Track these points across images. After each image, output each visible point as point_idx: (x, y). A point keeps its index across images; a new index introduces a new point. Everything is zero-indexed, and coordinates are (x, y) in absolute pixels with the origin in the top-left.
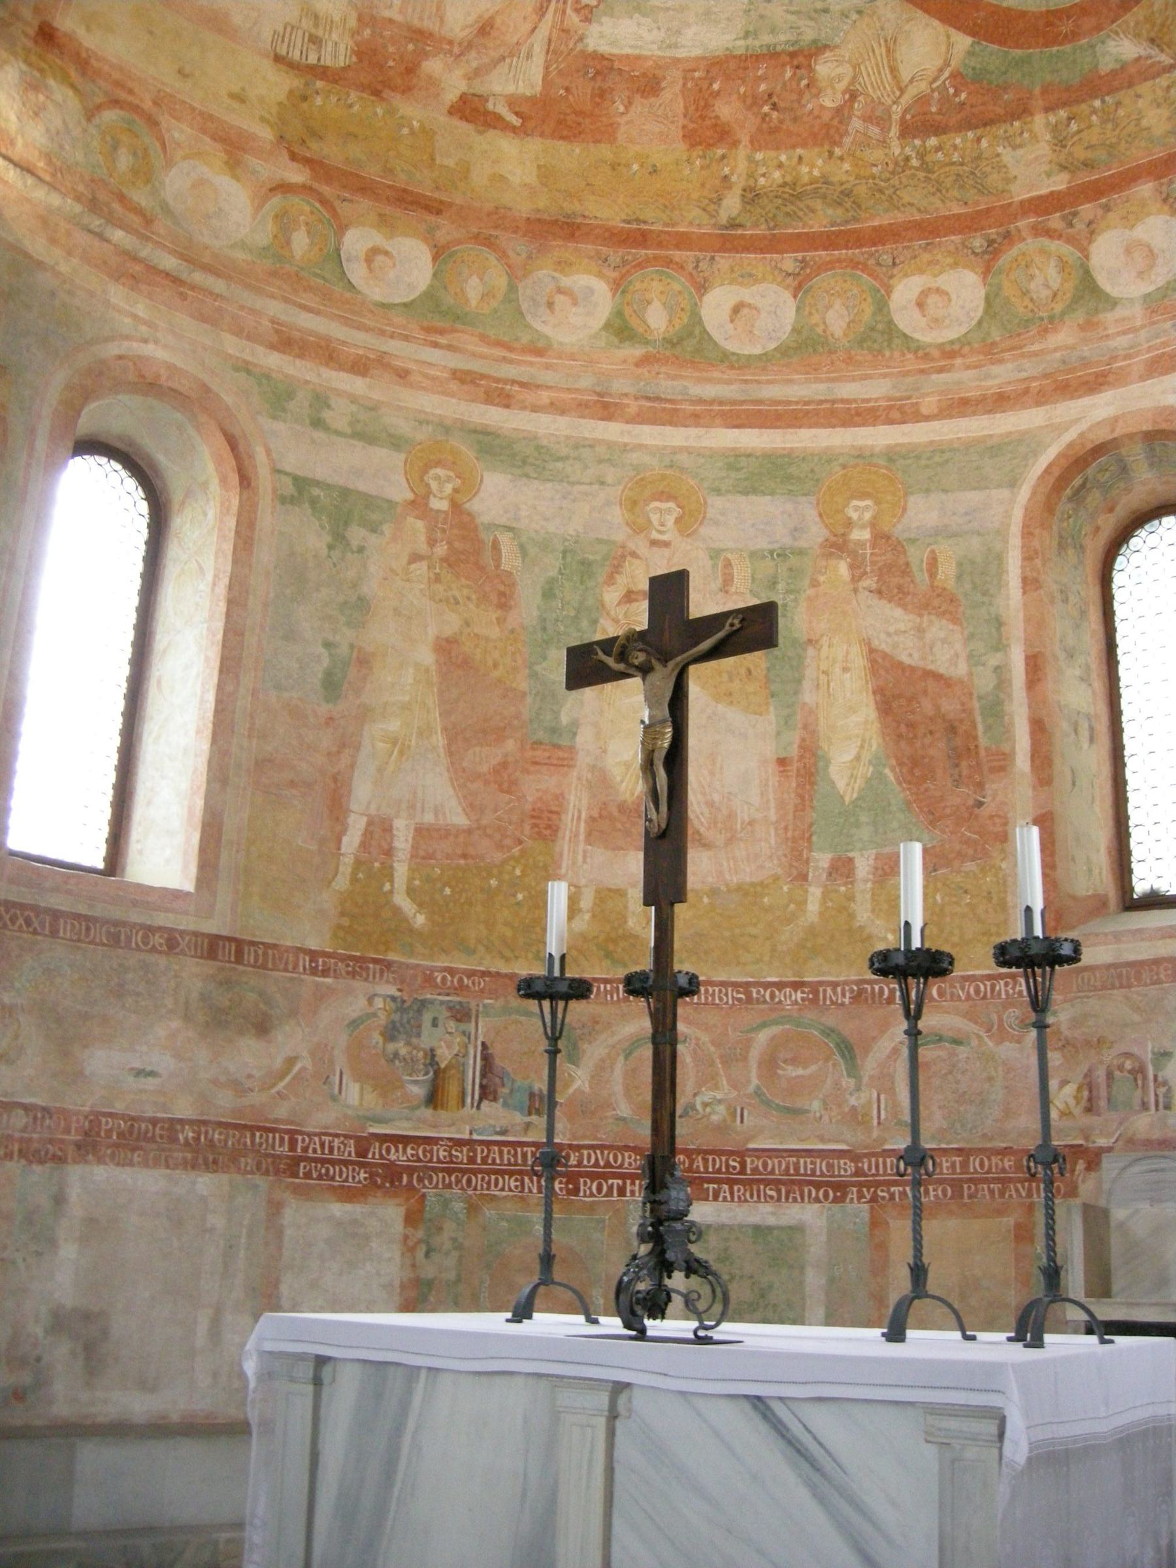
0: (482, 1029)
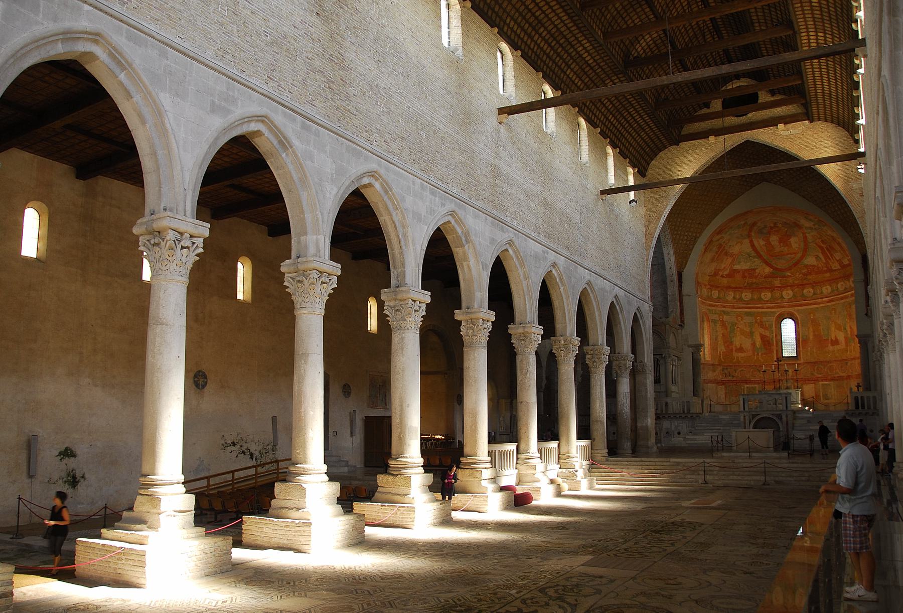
0: (729, 370)
